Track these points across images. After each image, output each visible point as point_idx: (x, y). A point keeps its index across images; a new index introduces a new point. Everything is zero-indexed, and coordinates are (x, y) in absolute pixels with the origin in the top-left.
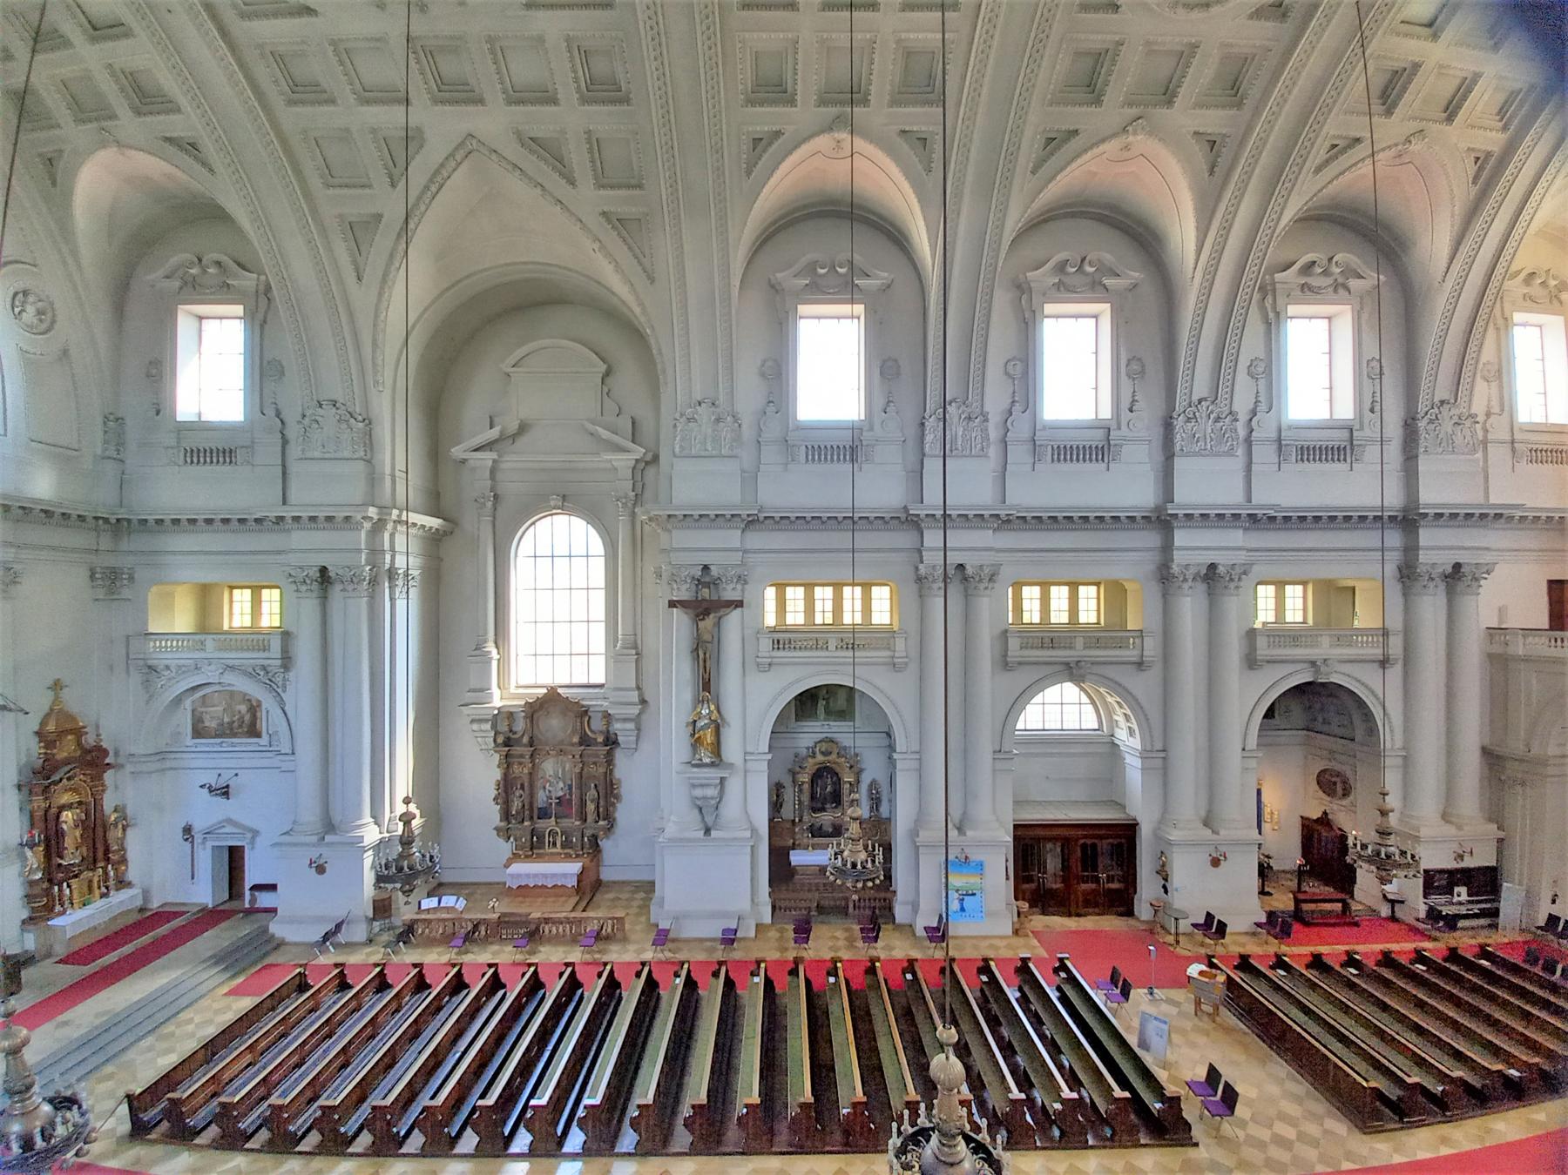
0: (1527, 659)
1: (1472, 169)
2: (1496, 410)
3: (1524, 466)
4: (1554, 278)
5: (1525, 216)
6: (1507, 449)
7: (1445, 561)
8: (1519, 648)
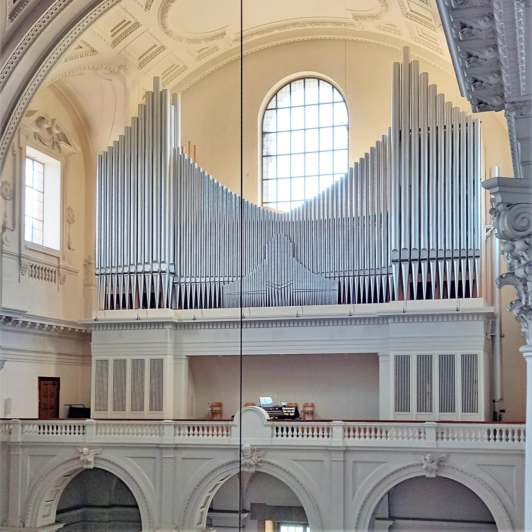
0: (23, 445)
2: (9, 225)
3: (26, 278)
4: (58, 128)
5: (44, 67)
6: (15, 262)
8: (18, 437)
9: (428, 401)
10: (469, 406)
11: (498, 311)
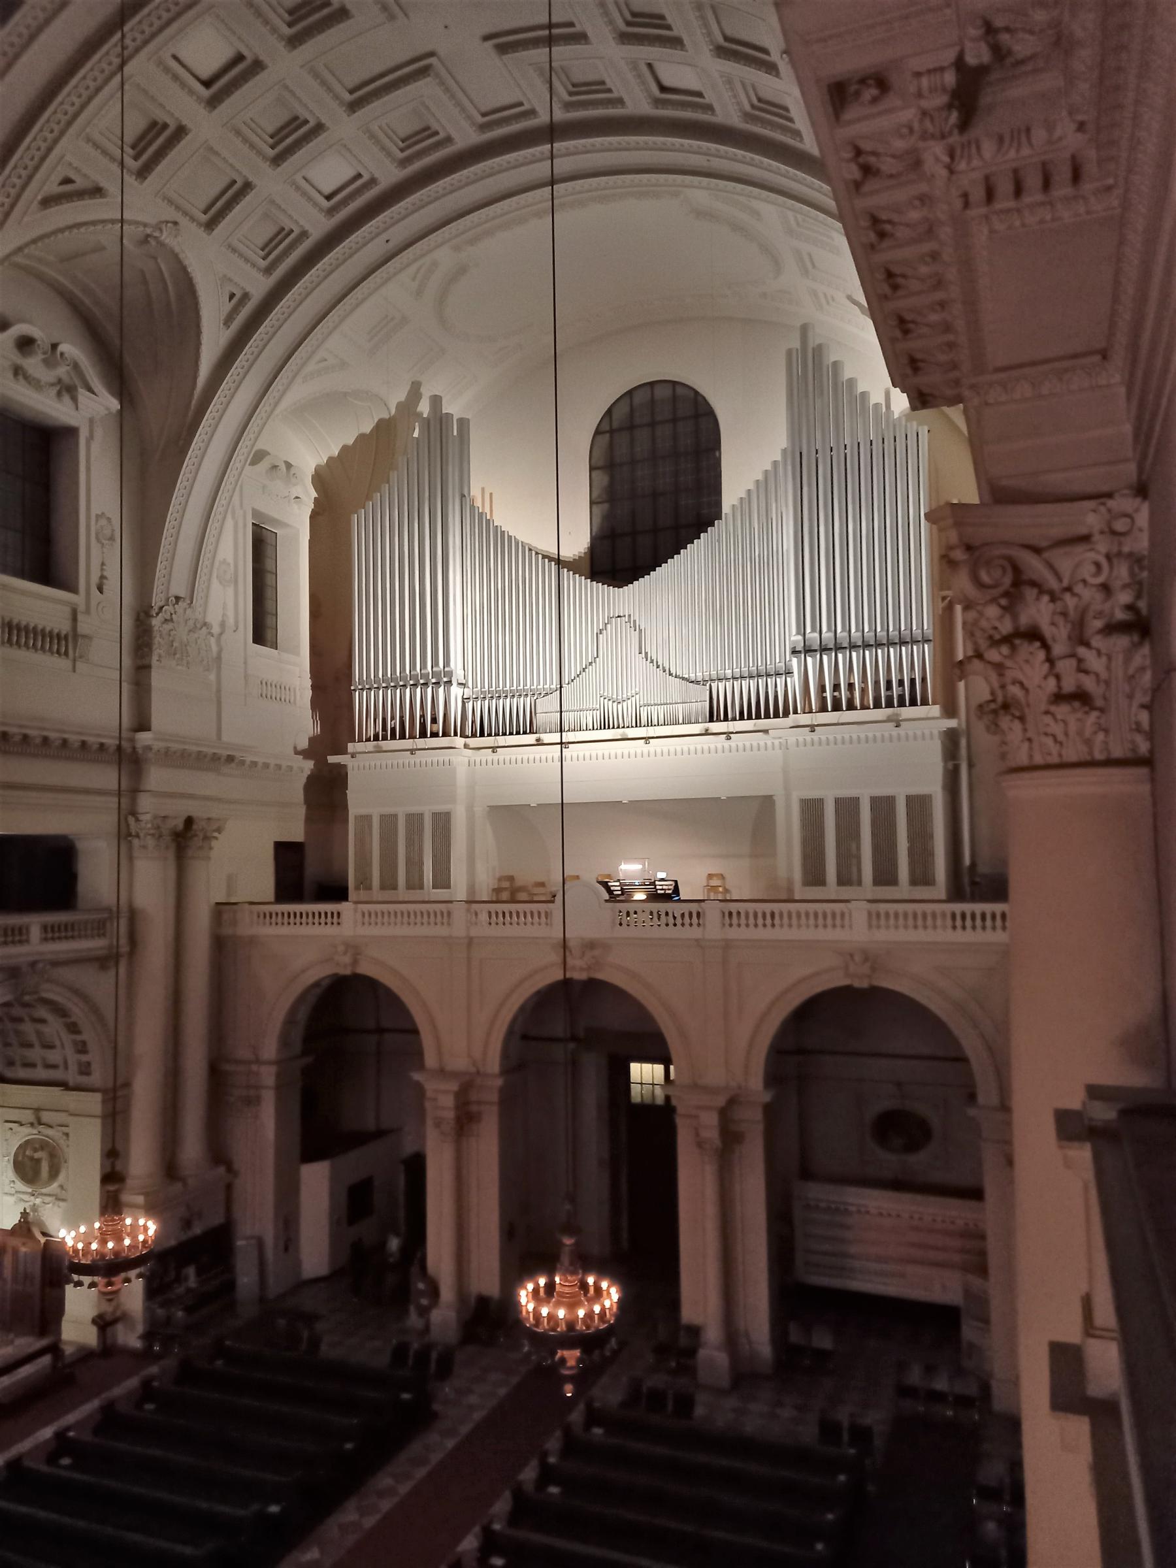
1: (228, 307)
7: (179, 810)
9: (854, 869)
10: (921, 877)
11: (964, 726)
